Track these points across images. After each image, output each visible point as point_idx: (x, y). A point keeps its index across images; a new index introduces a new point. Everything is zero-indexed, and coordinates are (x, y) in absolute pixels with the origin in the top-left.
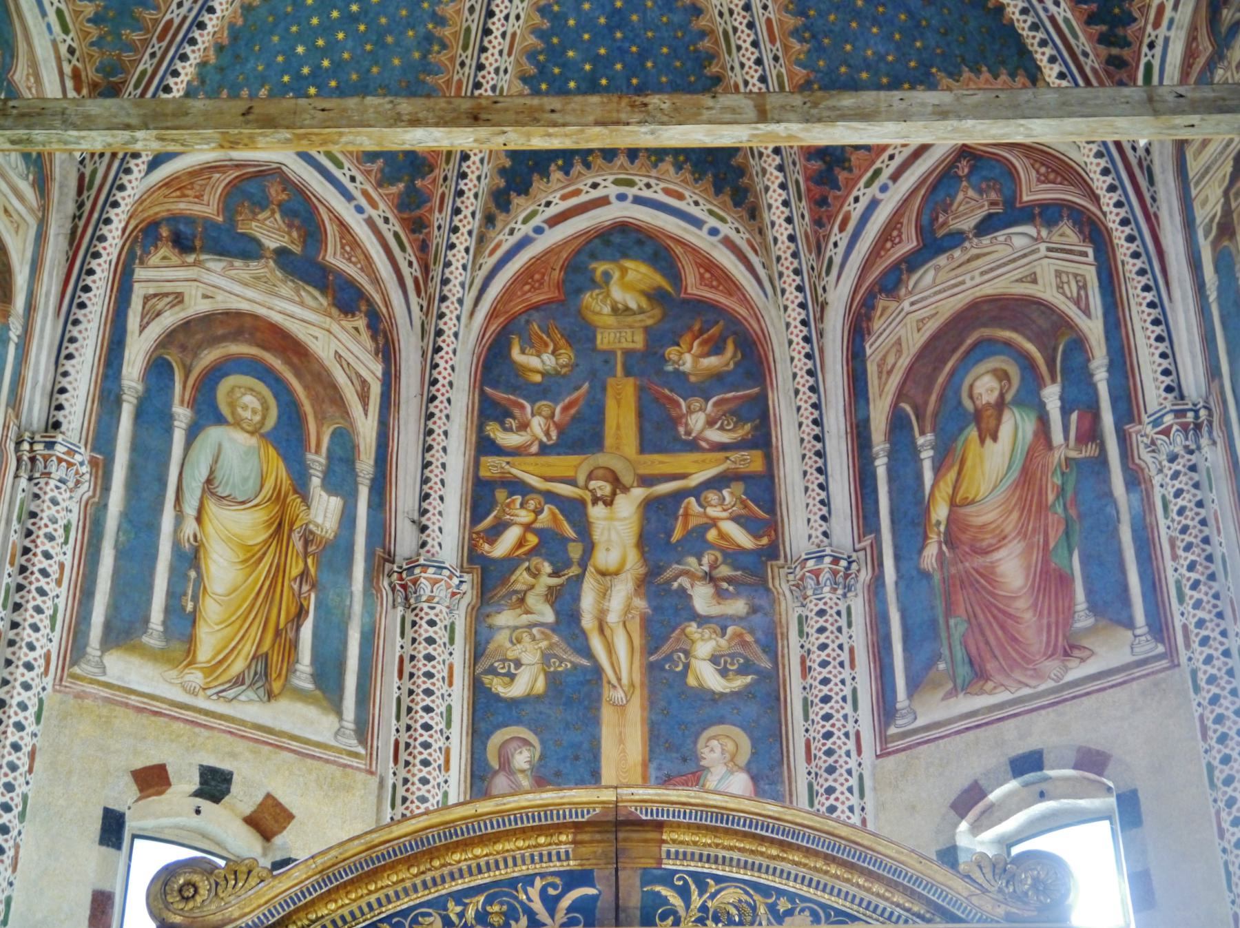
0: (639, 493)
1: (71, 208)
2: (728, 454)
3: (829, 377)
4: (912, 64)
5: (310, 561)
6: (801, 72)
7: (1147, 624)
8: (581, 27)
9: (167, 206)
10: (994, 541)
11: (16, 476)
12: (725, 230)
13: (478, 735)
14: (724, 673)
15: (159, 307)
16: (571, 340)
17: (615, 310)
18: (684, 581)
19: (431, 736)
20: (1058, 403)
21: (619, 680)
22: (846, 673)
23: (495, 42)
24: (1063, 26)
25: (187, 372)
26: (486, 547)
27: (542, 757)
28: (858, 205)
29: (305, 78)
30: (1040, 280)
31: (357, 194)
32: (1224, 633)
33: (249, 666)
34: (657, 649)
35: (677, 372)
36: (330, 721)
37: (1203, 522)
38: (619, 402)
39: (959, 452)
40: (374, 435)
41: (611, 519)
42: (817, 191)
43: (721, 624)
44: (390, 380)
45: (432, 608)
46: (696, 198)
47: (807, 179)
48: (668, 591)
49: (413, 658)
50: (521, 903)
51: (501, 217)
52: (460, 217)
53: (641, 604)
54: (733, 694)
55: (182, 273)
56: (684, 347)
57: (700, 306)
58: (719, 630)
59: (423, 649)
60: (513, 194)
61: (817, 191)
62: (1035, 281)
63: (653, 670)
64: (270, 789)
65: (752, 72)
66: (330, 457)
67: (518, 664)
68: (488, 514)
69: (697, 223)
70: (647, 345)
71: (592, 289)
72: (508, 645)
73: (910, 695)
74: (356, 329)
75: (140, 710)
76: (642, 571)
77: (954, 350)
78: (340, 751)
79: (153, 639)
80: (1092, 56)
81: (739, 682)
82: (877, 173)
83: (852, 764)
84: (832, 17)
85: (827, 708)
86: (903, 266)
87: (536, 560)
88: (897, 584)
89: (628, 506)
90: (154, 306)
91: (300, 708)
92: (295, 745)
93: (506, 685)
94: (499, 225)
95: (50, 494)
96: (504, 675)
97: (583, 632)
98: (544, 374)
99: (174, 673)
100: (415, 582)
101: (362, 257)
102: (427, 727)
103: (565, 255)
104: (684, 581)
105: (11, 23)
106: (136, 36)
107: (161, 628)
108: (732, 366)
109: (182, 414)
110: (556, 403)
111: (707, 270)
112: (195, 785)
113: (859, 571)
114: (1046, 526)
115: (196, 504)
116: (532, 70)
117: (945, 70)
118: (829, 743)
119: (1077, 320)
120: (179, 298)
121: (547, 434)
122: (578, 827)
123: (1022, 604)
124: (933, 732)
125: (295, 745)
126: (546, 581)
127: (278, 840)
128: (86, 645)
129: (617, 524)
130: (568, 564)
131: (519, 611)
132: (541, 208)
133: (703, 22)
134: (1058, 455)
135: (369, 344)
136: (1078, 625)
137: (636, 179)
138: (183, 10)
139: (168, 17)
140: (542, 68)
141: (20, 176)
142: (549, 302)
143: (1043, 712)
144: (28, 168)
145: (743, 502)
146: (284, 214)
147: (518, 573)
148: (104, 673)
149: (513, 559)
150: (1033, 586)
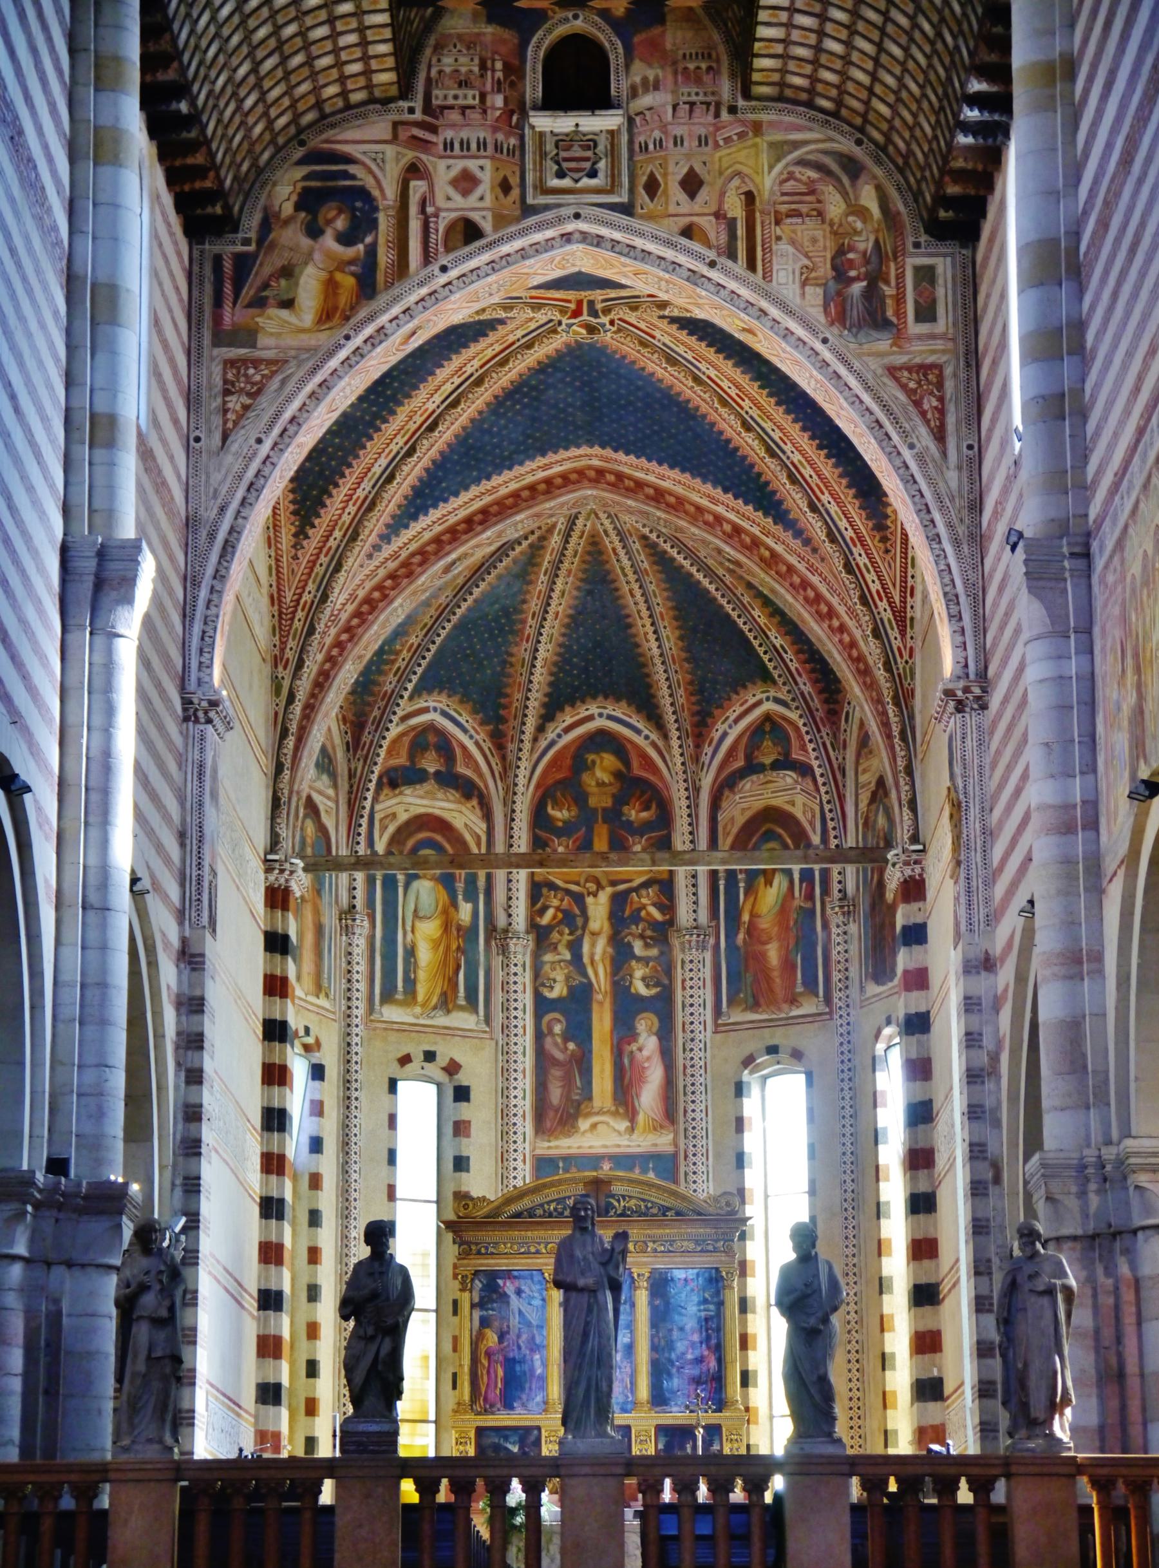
0: (609, 890)
1: (346, 787)
13: (538, 1016)
14: (647, 986)
18: (630, 938)
22: (701, 992)
23: (538, 670)
41: (596, 904)
43: (645, 961)
53: (610, 950)
54: (652, 997)
57: (640, 780)
59: (512, 979)
69: (638, 732)
79: (399, 996)
81: (654, 991)
89: (604, 897)
98: (564, 822)
104: (630, 938)
106: (371, 699)
116: (555, 670)
124: (735, 1027)
126: (567, 938)
130: (576, 929)
133: (640, 650)
135: (478, 811)
142: (565, 778)
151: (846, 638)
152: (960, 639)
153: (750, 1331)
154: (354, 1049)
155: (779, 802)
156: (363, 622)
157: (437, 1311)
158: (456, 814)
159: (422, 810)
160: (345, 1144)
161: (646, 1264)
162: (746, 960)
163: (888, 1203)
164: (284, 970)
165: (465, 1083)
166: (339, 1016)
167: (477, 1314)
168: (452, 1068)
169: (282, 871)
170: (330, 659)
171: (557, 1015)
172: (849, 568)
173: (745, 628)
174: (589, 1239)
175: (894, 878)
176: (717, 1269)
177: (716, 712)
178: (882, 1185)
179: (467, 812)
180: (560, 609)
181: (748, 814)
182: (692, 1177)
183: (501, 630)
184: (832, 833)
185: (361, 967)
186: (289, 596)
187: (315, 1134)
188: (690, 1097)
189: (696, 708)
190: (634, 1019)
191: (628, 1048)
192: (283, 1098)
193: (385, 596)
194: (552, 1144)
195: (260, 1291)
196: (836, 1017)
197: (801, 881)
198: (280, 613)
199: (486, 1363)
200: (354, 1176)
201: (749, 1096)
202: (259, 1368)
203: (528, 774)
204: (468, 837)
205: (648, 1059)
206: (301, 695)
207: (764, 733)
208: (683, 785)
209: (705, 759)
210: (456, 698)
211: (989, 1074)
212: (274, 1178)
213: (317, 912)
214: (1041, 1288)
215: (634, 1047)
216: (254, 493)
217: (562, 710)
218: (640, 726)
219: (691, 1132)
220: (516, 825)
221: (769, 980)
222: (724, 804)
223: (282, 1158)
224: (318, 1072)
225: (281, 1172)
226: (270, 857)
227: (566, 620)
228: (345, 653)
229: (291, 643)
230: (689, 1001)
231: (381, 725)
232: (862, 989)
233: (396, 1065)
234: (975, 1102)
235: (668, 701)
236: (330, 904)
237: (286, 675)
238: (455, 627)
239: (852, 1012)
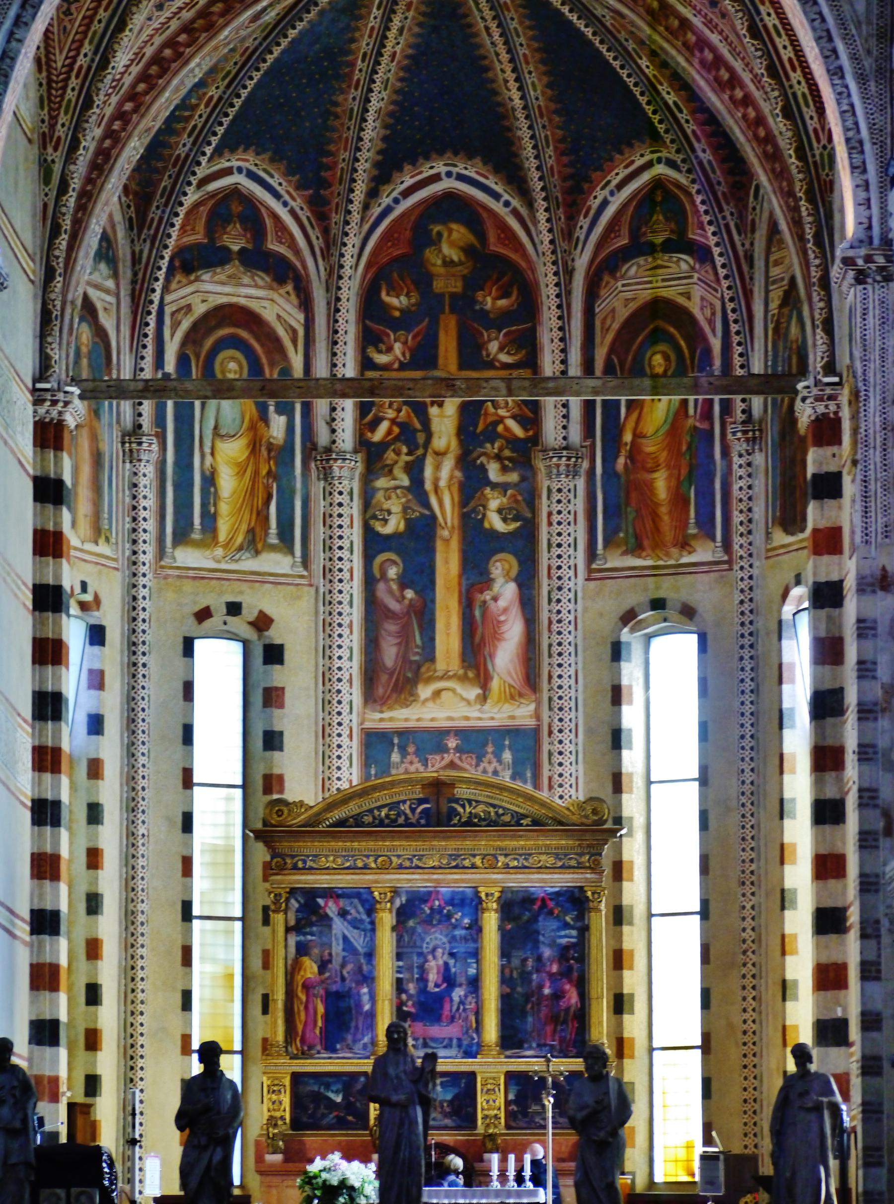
1: (129, 274)
3: (573, 323)
6: (560, 133)
11: (124, 462)
13: (368, 557)
14: (505, 520)
16: (416, 283)
22: (571, 529)
25: (198, 357)
26: (369, 434)
27: (404, 570)
31: (283, 193)
32: (751, 566)
35: (482, 309)
37: (750, 499)
38: (446, 332)
41: (442, 416)
43: (503, 488)
44: (309, 324)
47: (563, 194)
49: (331, 516)
53: (458, 474)
54: (509, 533)
56: (487, 291)
62: (689, 298)
69: (496, 196)
73: (605, 547)
75: (195, 578)
76: (459, 452)
79: (196, 536)
82: (609, 182)
83: (571, 584)
85: (559, 551)
86: (620, 255)
87: (399, 444)
89: (451, 406)
92: (271, 579)
98: (401, 311)
99: (208, 552)
100: (330, 467)
102: (340, 559)
103: (413, 218)
104: (483, 459)
106: (160, 165)
111: (503, 232)
112: (225, 611)
120: (189, 307)
121: (404, 354)
125: (271, 579)
127: (266, 633)
130: (417, 448)
133: (499, 99)
134: (690, 422)
142: (403, 256)
148: (175, 561)
151: (752, 113)
152: (863, 195)
153: (626, 946)
154: (141, 604)
155: (670, 293)
156: (151, 87)
157: (242, 919)
158: (266, 303)
159: (224, 300)
160: (131, 722)
161: (495, 882)
163: (793, 800)
164: (58, 523)
165: (278, 641)
166: (122, 563)
167: (293, 939)
168: (262, 623)
169: (54, 403)
170: (109, 134)
171: (393, 556)
172: (755, 31)
173: (630, 82)
174: (401, 1058)
175: (805, 414)
176: (581, 888)
177: (595, 175)
178: (786, 778)
179: (281, 301)
180: (398, 49)
181: (633, 306)
182: (557, 758)
184: (736, 339)
185: (149, 502)
186: (60, 60)
187: (94, 711)
188: (556, 660)
189: (569, 170)
191: (480, 597)
192: (58, 679)
193: (178, 55)
194: (386, 715)
195: (32, 911)
196: (736, 567)
198: (50, 81)
199: (303, 997)
200: (142, 760)
201: (629, 660)
202: (32, 1002)
203: (356, 251)
204: (281, 332)
205: (505, 610)
206: (76, 183)
207: (654, 203)
208: (552, 269)
209: (581, 234)
210: (266, 156)
211: (884, 710)
212: (48, 777)
213: (94, 438)
214: (810, 1105)
215: (487, 596)
216: (30, 11)
217: (400, 169)
218: (498, 188)
219: (556, 703)
220: (342, 317)
221: (655, 517)
222: (603, 292)
223: (57, 751)
224: (97, 635)
225: (56, 769)
226: (39, 386)
228: (130, 128)
229: (63, 118)
230: (556, 540)
231: (173, 197)
232: (768, 535)
233: (192, 620)
234: (866, 741)
235: (532, 163)
236: (110, 425)
237: (57, 157)
238: (266, 73)
239: (756, 564)
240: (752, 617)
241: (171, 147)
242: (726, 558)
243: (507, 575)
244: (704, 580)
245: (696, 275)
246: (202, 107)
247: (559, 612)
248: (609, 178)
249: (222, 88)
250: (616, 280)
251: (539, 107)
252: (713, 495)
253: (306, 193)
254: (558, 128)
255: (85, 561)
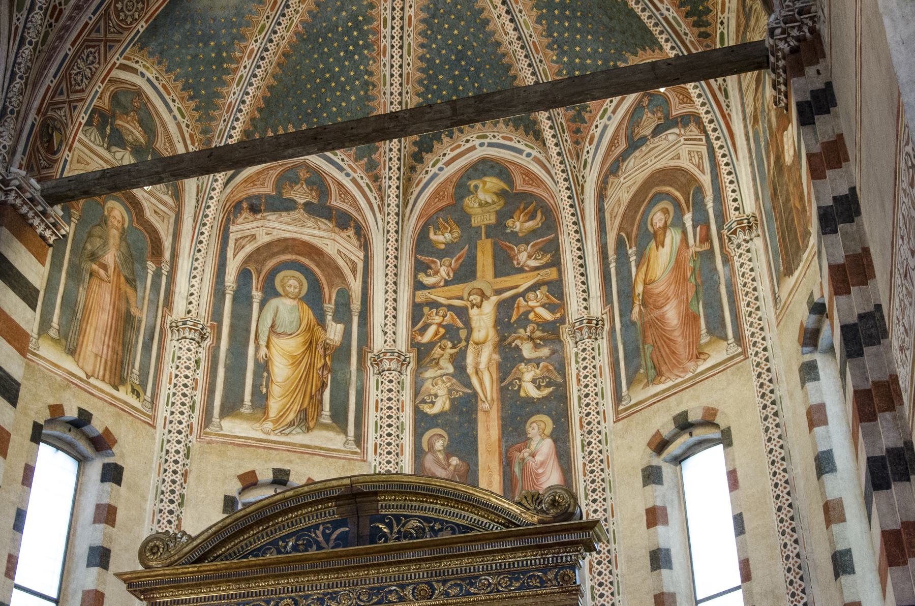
0: (494, 299)
1: (194, 202)
2: (538, 272)
4: (612, 51)
5: (327, 358)
7: (734, 337)
8: (443, 63)
9: (246, 192)
10: (664, 301)
12: (534, 153)
13: (418, 435)
14: (539, 388)
15: (243, 244)
16: (458, 223)
17: (481, 205)
18: (518, 342)
19: (392, 439)
20: (691, 223)
21: (486, 398)
24: (672, 21)
25: (259, 273)
26: (419, 338)
28: (598, 129)
29: (310, 114)
30: (681, 157)
31: (346, 167)
32: (764, 339)
33: (297, 416)
34: (505, 379)
35: (512, 231)
36: (341, 438)
37: (754, 280)
38: (483, 252)
39: (647, 256)
40: (360, 289)
42: (574, 126)
43: (537, 362)
45: (391, 374)
46: (518, 139)
48: (510, 348)
50: (313, 538)
51: (419, 167)
52: (392, 171)
53: (496, 357)
54: (543, 398)
55: (255, 224)
58: (536, 366)
60: (424, 154)
61: (574, 126)
62: (679, 158)
63: (503, 391)
64: (310, 476)
65: (527, 71)
66: (336, 304)
67: (436, 396)
68: (419, 321)
69: (520, 152)
70: (497, 220)
71: (469, 196)
72: (431, 387)
73: (628, 389)
74: (349, 236)
75: (239, 445)
76: (497, 339)
77: (644, 201)
78: (347, 452)
79: (246, 409)
80: (690, 34)
81: (546, 392)
82: (605, 111)
84: (566, 35)
85: (587, 400)
87: (444, 342)
88: (621, 329)
89: (489, 307)
90: (240, 243)
91: (325, 433)
92: (322, 452)
93: (430, 408)
94: (419, 171)
95: (187, 346)
96: (429, 403)
97: (468, 376)
98: (446, 244)
99: (258, 425)
100: (381, 361)
101: (351, 199)
103: (455, 180)
104: (518, 342)
105: (153, 120)
107: (250, 404)
108: (540, 225)
109: (257, 295)
110: (452, 259)
113: (604, 325)
114: (687, 290)
115: (266, 339)
116: (422, 89)
117: (629, 52)
118: (589, 419)
119: (698, 176)
120: (253, 237)
121: (448, 275)
122: (337, 498)
123: (677, 333)
125: (322, 452)
128: (212, 417)
129: (483, 316)
130: (460, 341)
131: (436, 369)
132: (441, 158)
133: (502, 50)
135: (356, 243)
136: (702, 341)
137: (488, 134)
138: (236, 96)
139: (229, 101)
140: (427, 88)
141: (164, 193)
142: (447, 206)
143: (687, 390)
144: (168, 188)
145: (547, 296)
146: (307, 184)
147: (435, 349)
149: (433, 342)
150: (681, 323)
159: (288, 235)
162: (644, 331)
179: (341, 241)
181: (634, 189)
183: (356, 45)
190: (526, 422)
191: (518, 456)
196: (751, 351)
197: (694, 227)
204: (341, 262)
205: (542, 464)
215: (526, 453)
221: (669, 341)
227: (422, 27)
240: (772, 386)
241: (224, 97)
242: (740, 350)
243: (542, 434)
244: (719, 381)
245: (682, 139)
246: (246, 59)
247: (591, 453)
248: (605, 106)
249: (259, 41)
250: (618, 177)
251: (534, 42)
252: (720, 300)
253: (362, 162)
254: (553, 61)
255: (79, 387)
